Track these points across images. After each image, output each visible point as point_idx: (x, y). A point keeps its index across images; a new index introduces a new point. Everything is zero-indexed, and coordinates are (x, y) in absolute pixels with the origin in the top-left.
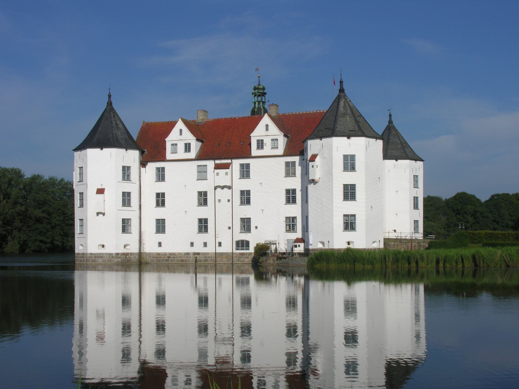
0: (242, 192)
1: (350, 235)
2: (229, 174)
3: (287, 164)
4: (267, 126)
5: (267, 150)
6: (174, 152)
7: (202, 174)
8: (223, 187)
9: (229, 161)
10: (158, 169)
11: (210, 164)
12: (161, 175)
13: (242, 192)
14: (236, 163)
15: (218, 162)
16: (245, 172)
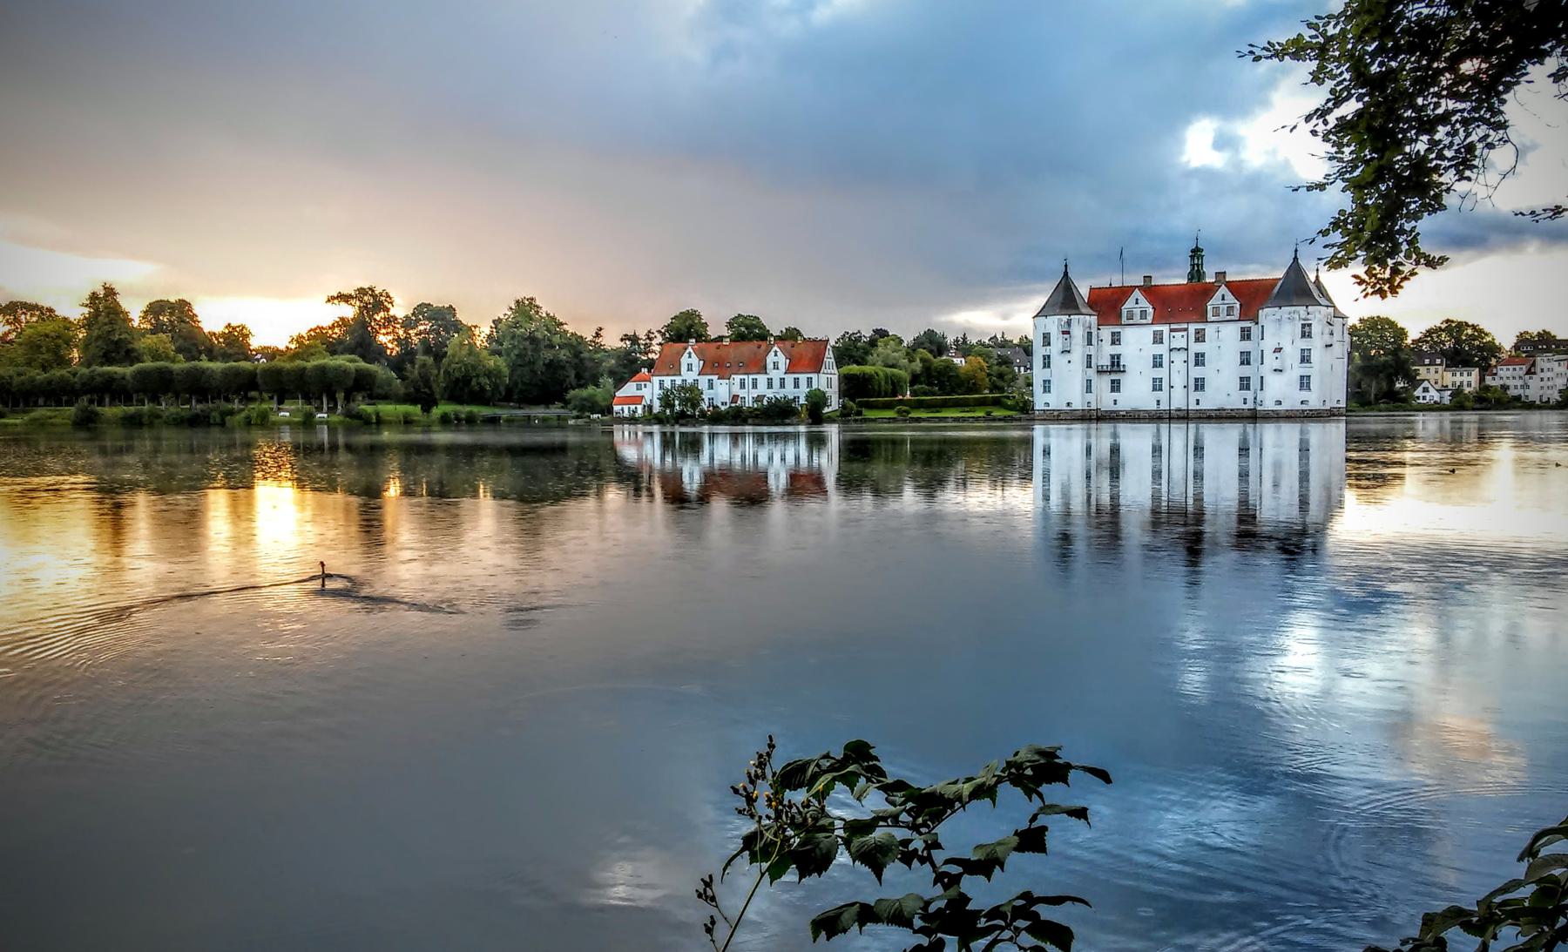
0: (1197, 355)
1: (1304, 395)
2: (1186, 337)
3: (1243, 330)
4: (1223, 296)
5: (1223, 316)
6: (1130, 317)
7: (1158, 339)
8: (1179, 350)
9: (1185, 326)
10: (1113, 334)
11: (1165, 328)
12: (1116, 339)
13: (1197, 355)
14: (1192, 327)
15: (1173, 326)
16: (1200, 337)
